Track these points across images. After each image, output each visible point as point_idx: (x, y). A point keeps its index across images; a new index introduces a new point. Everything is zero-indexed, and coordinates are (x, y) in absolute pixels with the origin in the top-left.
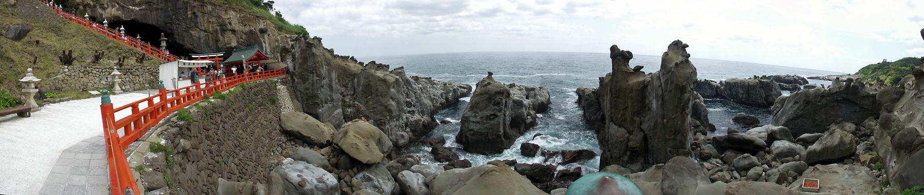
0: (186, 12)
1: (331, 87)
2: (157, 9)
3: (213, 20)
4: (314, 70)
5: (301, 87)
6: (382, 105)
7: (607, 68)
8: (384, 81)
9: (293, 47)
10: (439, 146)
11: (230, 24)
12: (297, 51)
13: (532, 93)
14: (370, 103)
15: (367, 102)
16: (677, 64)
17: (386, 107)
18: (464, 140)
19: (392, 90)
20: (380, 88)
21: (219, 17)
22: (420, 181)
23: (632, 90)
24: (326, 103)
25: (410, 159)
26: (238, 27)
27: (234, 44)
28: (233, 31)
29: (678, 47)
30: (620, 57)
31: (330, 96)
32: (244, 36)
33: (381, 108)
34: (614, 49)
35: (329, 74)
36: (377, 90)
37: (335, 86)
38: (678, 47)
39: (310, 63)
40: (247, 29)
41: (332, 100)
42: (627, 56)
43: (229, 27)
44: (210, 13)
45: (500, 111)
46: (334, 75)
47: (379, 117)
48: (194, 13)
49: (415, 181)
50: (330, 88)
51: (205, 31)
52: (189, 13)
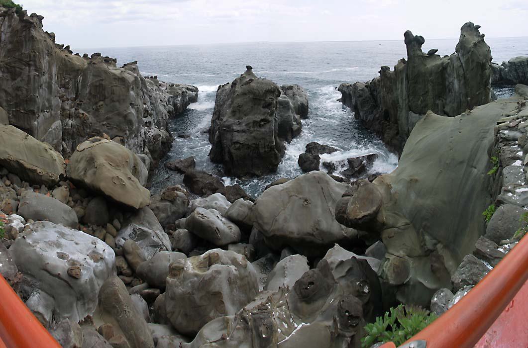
1: (50, 87)
6: (119, 114)
7: (402, 53)
14: (102, 111)
15: (97, 110)
16: (475, 44)
18: (227, 158)
19: (132, 92)
20: (117, 90)
23: (431, 74)
24: (43, 111)
29: (470, 29)
30: (413, 42)
31: (49, 101)
33: (117, 119)
34: (407, 34)
35: (50, 67)
36: (113, 93)
37: (55, 86)
38: (470, 29)
41: (50, 107)
42: (420, 41)
46: (54, 70)
50: (48, 93)
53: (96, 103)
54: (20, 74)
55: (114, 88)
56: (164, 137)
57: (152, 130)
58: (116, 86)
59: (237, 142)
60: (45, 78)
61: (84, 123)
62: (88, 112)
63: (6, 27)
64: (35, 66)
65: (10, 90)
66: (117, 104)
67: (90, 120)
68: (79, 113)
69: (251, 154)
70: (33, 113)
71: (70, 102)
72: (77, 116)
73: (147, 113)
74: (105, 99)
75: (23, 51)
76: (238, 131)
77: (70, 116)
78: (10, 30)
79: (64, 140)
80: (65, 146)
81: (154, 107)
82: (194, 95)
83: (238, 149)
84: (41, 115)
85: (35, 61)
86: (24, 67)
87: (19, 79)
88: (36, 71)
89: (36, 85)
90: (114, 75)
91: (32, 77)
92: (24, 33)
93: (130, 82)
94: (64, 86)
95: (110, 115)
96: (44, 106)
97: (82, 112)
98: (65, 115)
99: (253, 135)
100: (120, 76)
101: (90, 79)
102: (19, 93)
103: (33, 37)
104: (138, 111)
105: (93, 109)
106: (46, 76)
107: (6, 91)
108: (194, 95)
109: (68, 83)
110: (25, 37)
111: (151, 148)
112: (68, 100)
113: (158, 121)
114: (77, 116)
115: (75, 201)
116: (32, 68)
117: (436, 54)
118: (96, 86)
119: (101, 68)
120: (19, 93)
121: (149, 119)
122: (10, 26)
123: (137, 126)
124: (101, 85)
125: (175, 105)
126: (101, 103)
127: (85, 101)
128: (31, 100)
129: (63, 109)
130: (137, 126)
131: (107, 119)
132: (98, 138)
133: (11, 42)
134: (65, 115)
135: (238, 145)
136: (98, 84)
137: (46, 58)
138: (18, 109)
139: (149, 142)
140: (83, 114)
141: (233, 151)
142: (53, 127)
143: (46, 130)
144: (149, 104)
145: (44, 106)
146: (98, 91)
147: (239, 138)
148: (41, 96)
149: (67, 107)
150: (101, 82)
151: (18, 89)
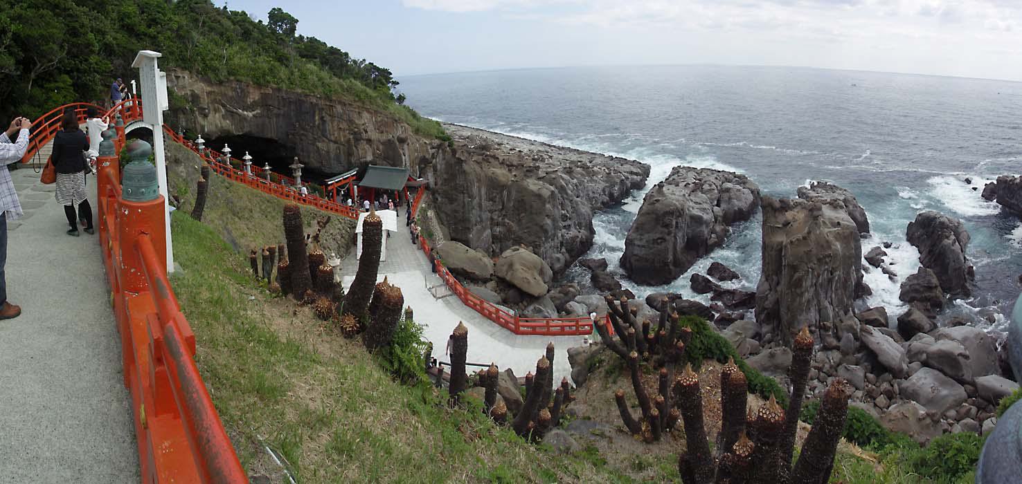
0: (314, 116)
1: (480, 206)
2: (278, 116)
3: (344, 125)
4: (466, 190)
5: (448, 208)
6: (537, 224)
8: (539, 196)
9: (433, 156)
10: (599, 271)
11: (366, 132)
12: (439, 162)
13: (725, 196)
15: (520, 220)
17: (542, 227)
18: (628, 265)
20: (535, 204)
21: (351, 122)
22: (584, 311)
24: (476, 225)
25: (571, 289)
26: (374, 135)
27: (369, 158)
28: (369, 141)
31: (480, 216)
32: (381, 147)
35: (480, 191)
36: (531, 207)
37: (484, 203)
39: (460, 180)
40: (384, 137)
41: (481, 221)
43: (364, 135)
44: (341, 117)
45: (669, 234)
47: (532, 238)
48: (322, 118)
49: (581, 310)
50: (479, 206)
51: (335, 142)
52: (317, 118)
53: (519, 215)
54: (456, 200)
56: (584, 237)
57: (571, 232)
60: (476, 201)
61: (509, 230)
62: (513, 222)
63: (441, 158)
64: (468, 194)
65: (449, 213)
67: (514, 229)
68: (505, 222)
70: (469, 229)
71: (497, 213)
72: (504, 225)
73: (564, 218)
75: (457, 182)
76: (639, 246)
77: (498, 225)
78: (444, 162)
79: (493, 243)
80: (494, 247)
81: (575, 210)
82: (639, 180)
83: (638, 260)
84: (475, 228)
85: (467, 190)
87: (456, 204)
88: (470, 197)
89: (470, 208)
90: (532, 191)
91: (466, 203)
92: (457, 168)
93: (546, 197)
94: (492, 199)
95: (529, 225)
96: (476, 221)
97: (508, 221)
98: (494, 224)
100: (537, 193)
101: (514, 193)
102: (457, 215)
104: (554, 220)
106: (477, 198)
107: (446, 213)
108: (639, 180)
109: (496, 197)
110: (458, 170)
111: (569, 247)
112: (496, 211)
113: (579, 223)
114: (504, 225)
115: (501, 290)
116: (466, 195)
118: (519, 201)
120: (457, 215)
121: (569, 222)
122: (444, 159)
123: (553, 232)
124: (523, 200)
125: (611, 195)
126: (523, 214)
128: (465, 220)
129: (492, 219)
130: (553, 232)
131: (527, 228)
132: (517, 247)
133: (447, 173)
134: (494, 224)
137: (476, 184)
139: (566, 243)
140: (508, 223)
141: (632, 261)
142: (484, 235)
143: (479, 238)
144: (569, 209)
145: (476, 221)
148: (474, 215)
149: (495, 217)
151: (456, 211)
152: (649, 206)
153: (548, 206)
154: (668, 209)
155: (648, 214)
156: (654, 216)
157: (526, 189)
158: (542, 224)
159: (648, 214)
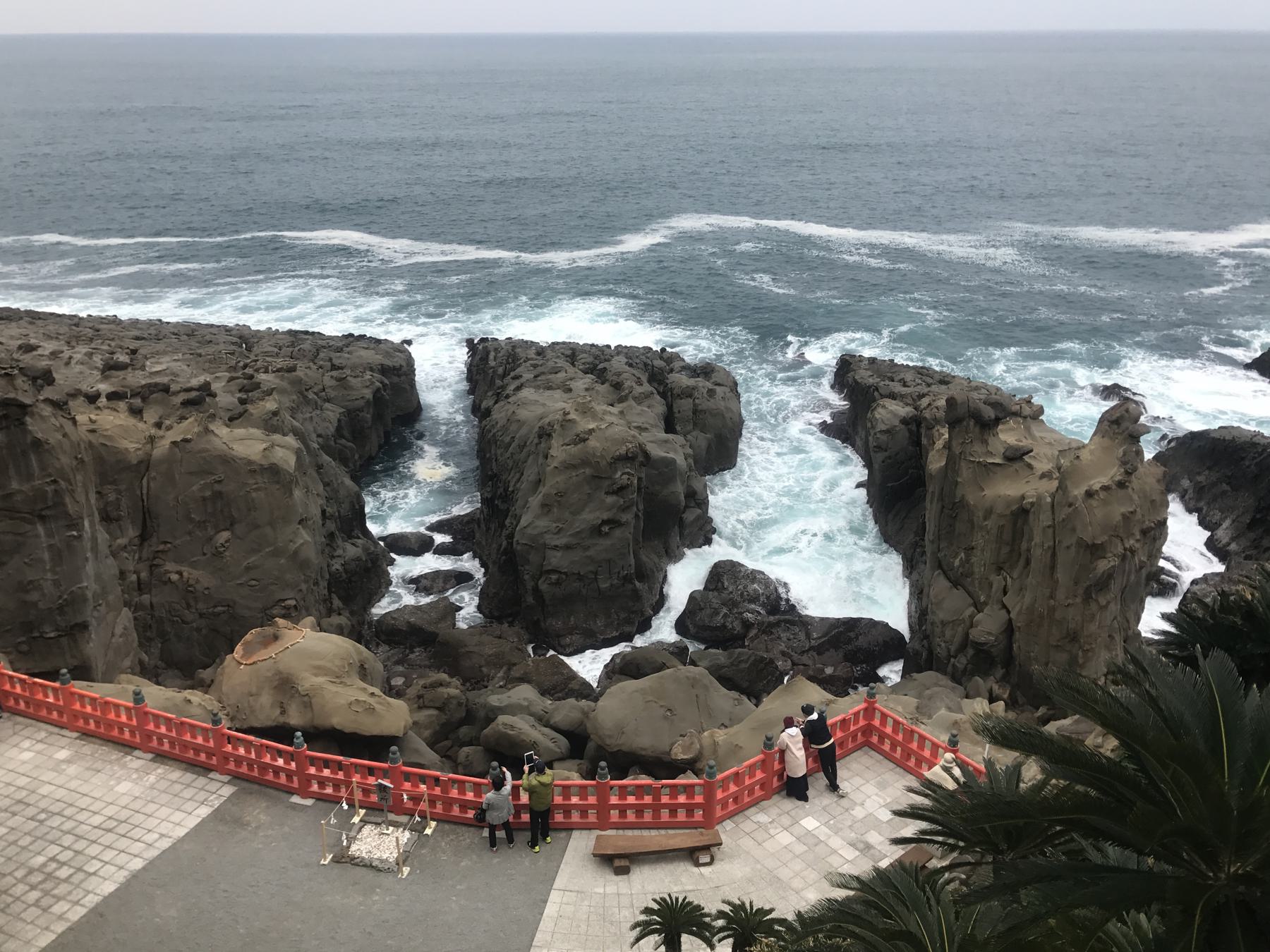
6: (277, 553)
8: (273, 471)
15: (218, 554)
55: (254, 495)
58: (257, 490)
59: (554, 571)
62: (193, 565)
66: (268, 530)
69: (584, 591)
74: (232, 525)
75: (15, 485)
76: (556, 548)
83: (558, 583)
86: (28, 527)
90: (250, 462)
99: (588, 553)
100: (264, 462)
102: (34, 596)
103: (38, 444)
105: (205, 554)
117: (1026, 458)
118: (204, 499)
119: (208, 450)
124: (218, 495)
126: (225, 535)
127: (178, 542)
131: (248, 569)
135: (554, 577)
136: (208, 493)
138: (36, 634)
141: (543, 586)
146: (210, 510)
147: (556, 559)
150: (217, 487)
152: (573, 449)
153: (298, 493)
154: (623, 450)
155: (574, 467)
156: (588, 471)
157: (227, 460)
158: (293, 547)
159: (574, 467)
